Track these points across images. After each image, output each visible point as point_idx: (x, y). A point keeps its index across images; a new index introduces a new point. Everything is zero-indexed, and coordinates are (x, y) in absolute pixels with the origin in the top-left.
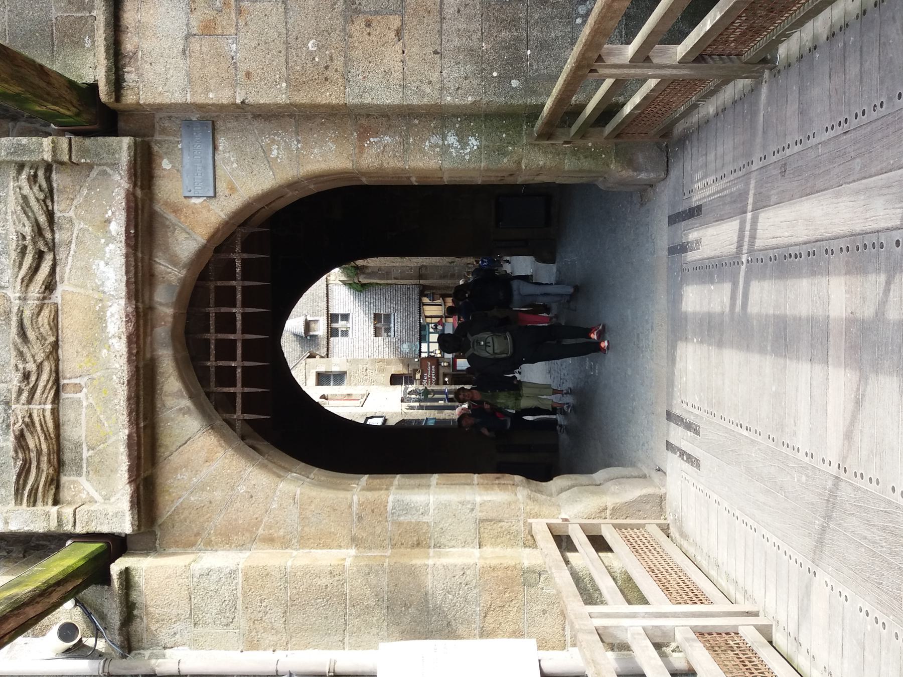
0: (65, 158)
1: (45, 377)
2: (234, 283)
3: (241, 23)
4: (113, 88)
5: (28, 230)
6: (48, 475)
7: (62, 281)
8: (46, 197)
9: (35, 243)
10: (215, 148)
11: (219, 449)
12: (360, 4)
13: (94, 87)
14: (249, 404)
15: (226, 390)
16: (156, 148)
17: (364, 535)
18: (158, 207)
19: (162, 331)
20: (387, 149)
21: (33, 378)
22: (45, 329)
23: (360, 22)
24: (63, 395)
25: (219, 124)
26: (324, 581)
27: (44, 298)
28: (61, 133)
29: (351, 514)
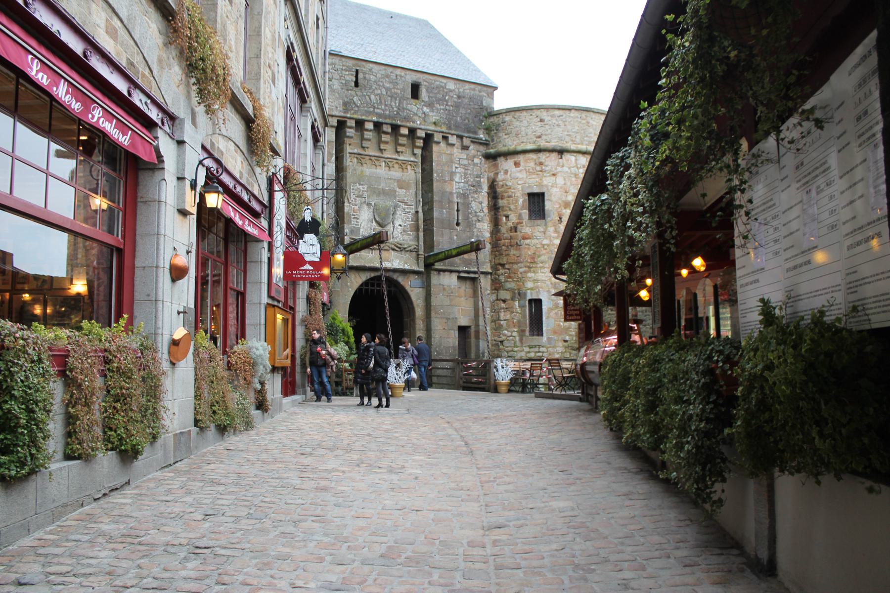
5: (406, 246)
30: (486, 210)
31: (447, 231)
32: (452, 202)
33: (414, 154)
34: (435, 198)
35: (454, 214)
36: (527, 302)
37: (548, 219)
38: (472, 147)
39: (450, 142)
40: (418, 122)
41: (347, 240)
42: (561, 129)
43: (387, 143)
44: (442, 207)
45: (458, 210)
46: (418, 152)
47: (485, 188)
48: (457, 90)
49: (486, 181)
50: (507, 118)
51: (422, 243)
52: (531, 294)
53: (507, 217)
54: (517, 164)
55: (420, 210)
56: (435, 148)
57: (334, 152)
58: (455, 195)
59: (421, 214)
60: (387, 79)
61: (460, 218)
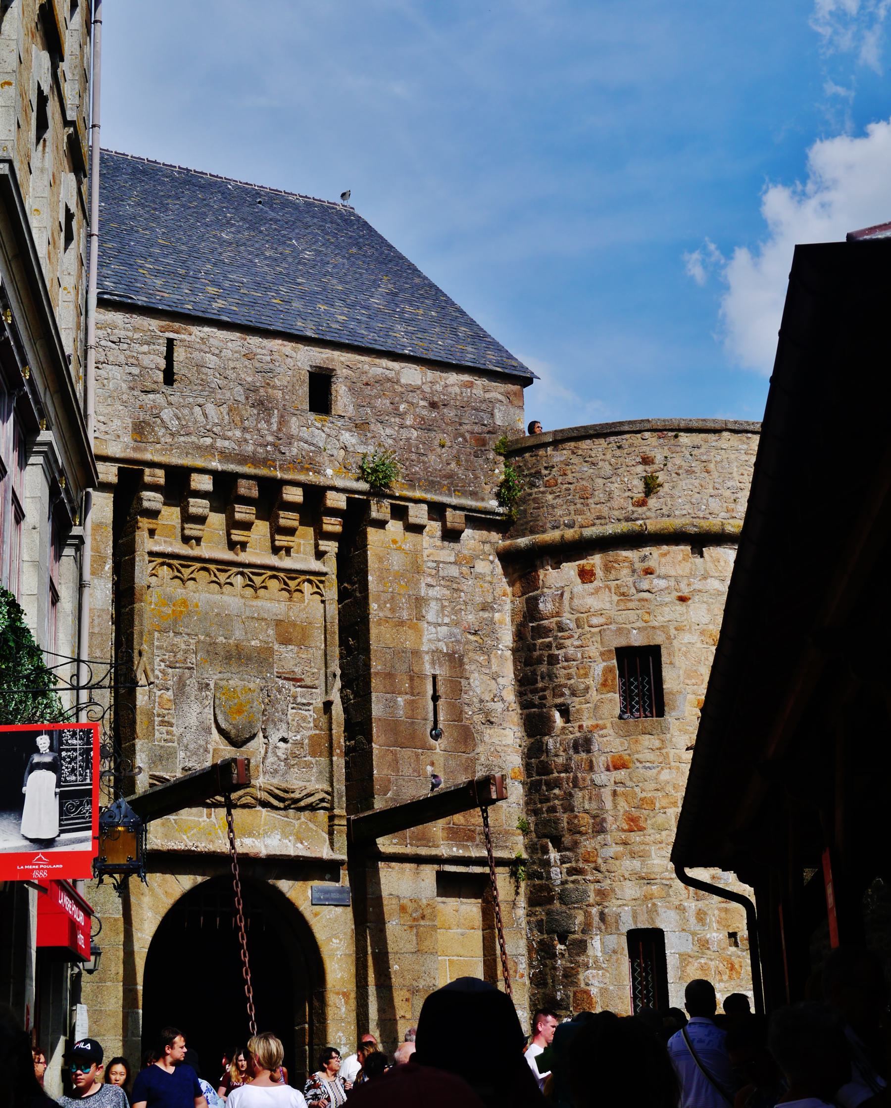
3: (406, 927)
7: (267, 811)
23: (408, 995)
28: (348, 820)
30: (510, 696)
31: (407, 753)
32: (422, 677)
34: (376, 666)
35: (425, 708)
36: (624, 940)
37: (670, 717)
38: (468, 533)
39: (412, 520)
40: (329, 472)
41: (142, 783)
42: (697, 483)
44: (394, 691)
45: (435, 698)
46: (331, 547)
47: (507, 637)
48: (426, 388)
49: (508, 619)
50: (557, 457)
51: (340, 786)
52: (635, 917)
53: (565, 712)
54: (586, 575)
55: (335, 696)
57: (110, 551)
58: (427, 658)
59: (338, 709)
61: (441, 717)
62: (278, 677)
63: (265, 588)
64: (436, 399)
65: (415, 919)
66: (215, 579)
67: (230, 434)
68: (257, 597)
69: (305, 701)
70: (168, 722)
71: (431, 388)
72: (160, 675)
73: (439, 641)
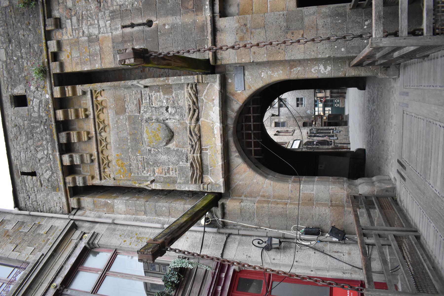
0: (201, 81)
1: (197, 146)
2: (250, 115)
3: (252, 36)
4: (214, 61)
5: (191, 104)
6: (199, 175)
7: (201, 118)
8: (196, 93)
9: (193, 107)
10: (244, 75)
11: (248, 168)
12: (290, 27)
13: (209, 60)
14: (256, 153)
15: (249, 148)
16: (227, 76)
17: (293, 196)
18: (228, 94)
19: (230, 132)
20: (300, 72)
21: (194, 147)
22: (197, 132)
24: (202, 151)
25: (246, 68)
26: (280, 210)
27: (196, 123)
29: (289, 190)
32: (123, 35)
33: (84, 93)
43: (79, 134)
46: (79, 88)
48: (5, 46)
56: (68, 69)
60: (19, 139)
62: (140, 113)
63: (104, 121)
64: (7, 40)
65: (247, 31)
66: (105, 148)
67: (45, 146)
68: (109, 125)
69: (148, 98)
70: (168, 170)
71: (4, 43)
72: (149, 173)
73: (106, 25)
